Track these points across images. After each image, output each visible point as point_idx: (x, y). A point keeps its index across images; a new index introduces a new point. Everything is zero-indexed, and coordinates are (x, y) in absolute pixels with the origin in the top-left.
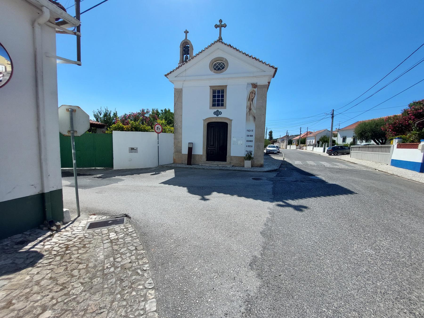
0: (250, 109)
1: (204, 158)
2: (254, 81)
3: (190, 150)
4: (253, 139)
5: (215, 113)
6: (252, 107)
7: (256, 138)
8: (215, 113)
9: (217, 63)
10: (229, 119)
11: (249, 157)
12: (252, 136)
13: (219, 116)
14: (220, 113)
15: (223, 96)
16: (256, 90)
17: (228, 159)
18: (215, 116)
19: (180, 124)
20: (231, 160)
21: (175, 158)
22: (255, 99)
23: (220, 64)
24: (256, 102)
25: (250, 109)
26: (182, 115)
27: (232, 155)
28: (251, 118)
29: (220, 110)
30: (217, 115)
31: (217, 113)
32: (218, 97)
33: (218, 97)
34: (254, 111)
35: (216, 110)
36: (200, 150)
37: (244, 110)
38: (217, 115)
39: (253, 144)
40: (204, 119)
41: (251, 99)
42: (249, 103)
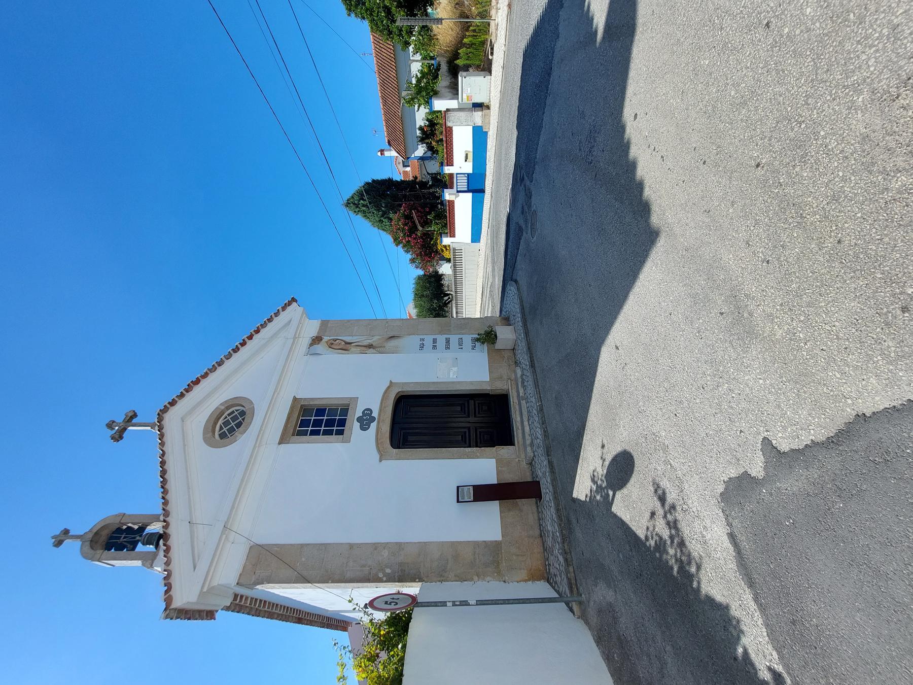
0: (370, 346)
1: (505, 451)
2: (305, 341)
3: (482, 493)
4: (441, 339)
5: (364, 427)
6: (366, 343)
7: (441, 333)
8: (364, 427)
9: (221, 428)
10: (389, 387)
11: (488, 337)
12: (435, 341)
13: (375, 414)
14: (368, 412)
15: (320, 411)
16: (326, 339)
17: (500, 386)
18: (374, 425)
19: (386, 553)
20: (501, 378)
21: (524, 574)
22: (348, 339)
23: (226, 423)
24: (355, 338)
25: (370, 346)
26: (351, 546)
27: (486, 377)
28: (393, 343)
29: (359, 413)
30: (373, 419)
31: (366, 420)
32: (319, 420)
33: (319, 420)
34: (374, 340)
35: (357, 425)
36: (483, 467)
37: (372, 358)
38: (373, 419)
39: (454, 339)
40: (378, 457)
41: (346, 347)
42: (353, 349)
